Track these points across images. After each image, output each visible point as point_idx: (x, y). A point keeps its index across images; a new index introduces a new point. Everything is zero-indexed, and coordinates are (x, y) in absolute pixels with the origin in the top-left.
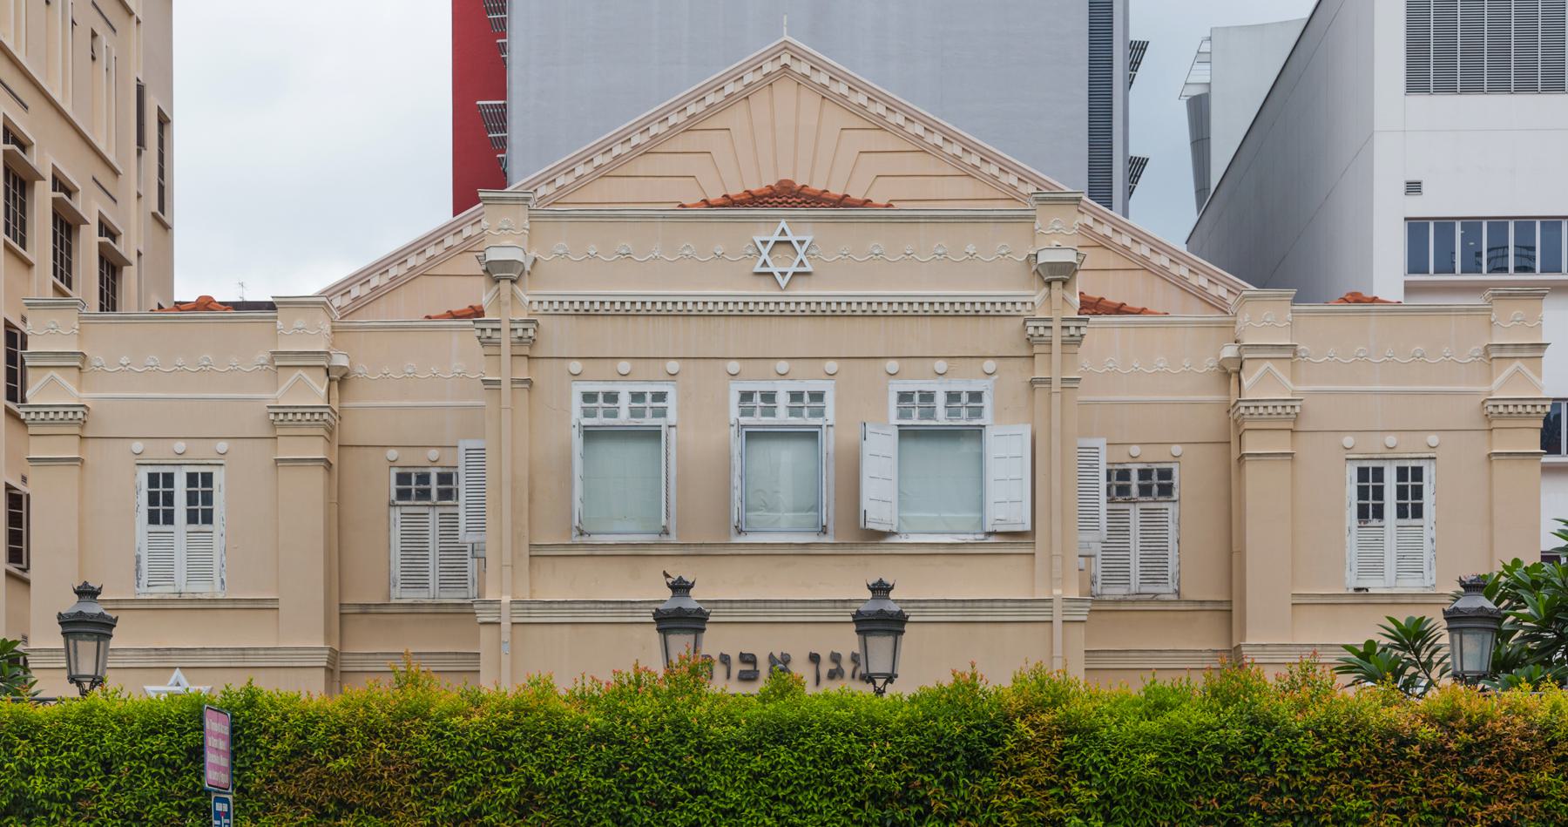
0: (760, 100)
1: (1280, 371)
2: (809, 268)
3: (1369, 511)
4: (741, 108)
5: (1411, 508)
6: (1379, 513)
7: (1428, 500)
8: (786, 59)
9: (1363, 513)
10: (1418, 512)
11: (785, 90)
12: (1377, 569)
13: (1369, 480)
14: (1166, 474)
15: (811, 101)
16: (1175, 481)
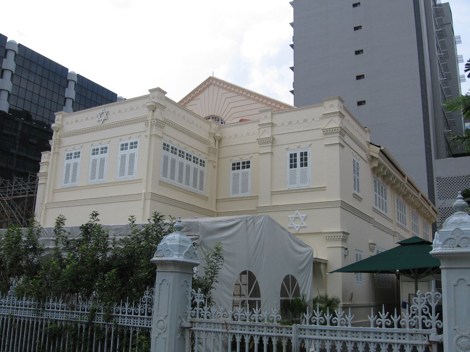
0: (206, 91)
1: (269, 129)
2: (106, 118)
3: (293, 165)
4: (202, 94)
5: (304, 164)
6: (295, 166)
7: (309, 162)
8: (211, 81)
9: (291, 167)
10: (306, 165)
11: (211, 87)
12: (293, 182)
13: (293, 157)
14: (248, 162)
15: (216, 88)
16: (251, 164)
